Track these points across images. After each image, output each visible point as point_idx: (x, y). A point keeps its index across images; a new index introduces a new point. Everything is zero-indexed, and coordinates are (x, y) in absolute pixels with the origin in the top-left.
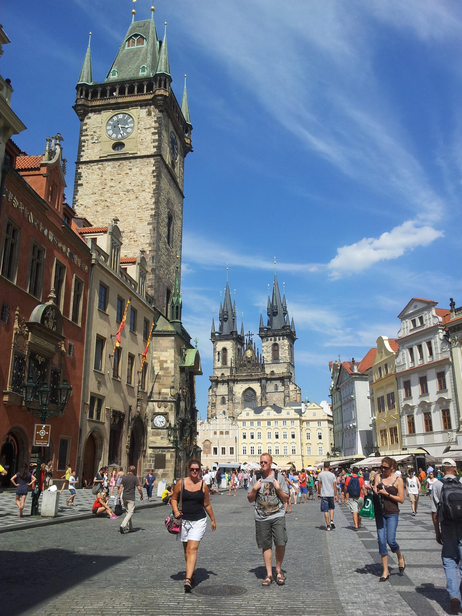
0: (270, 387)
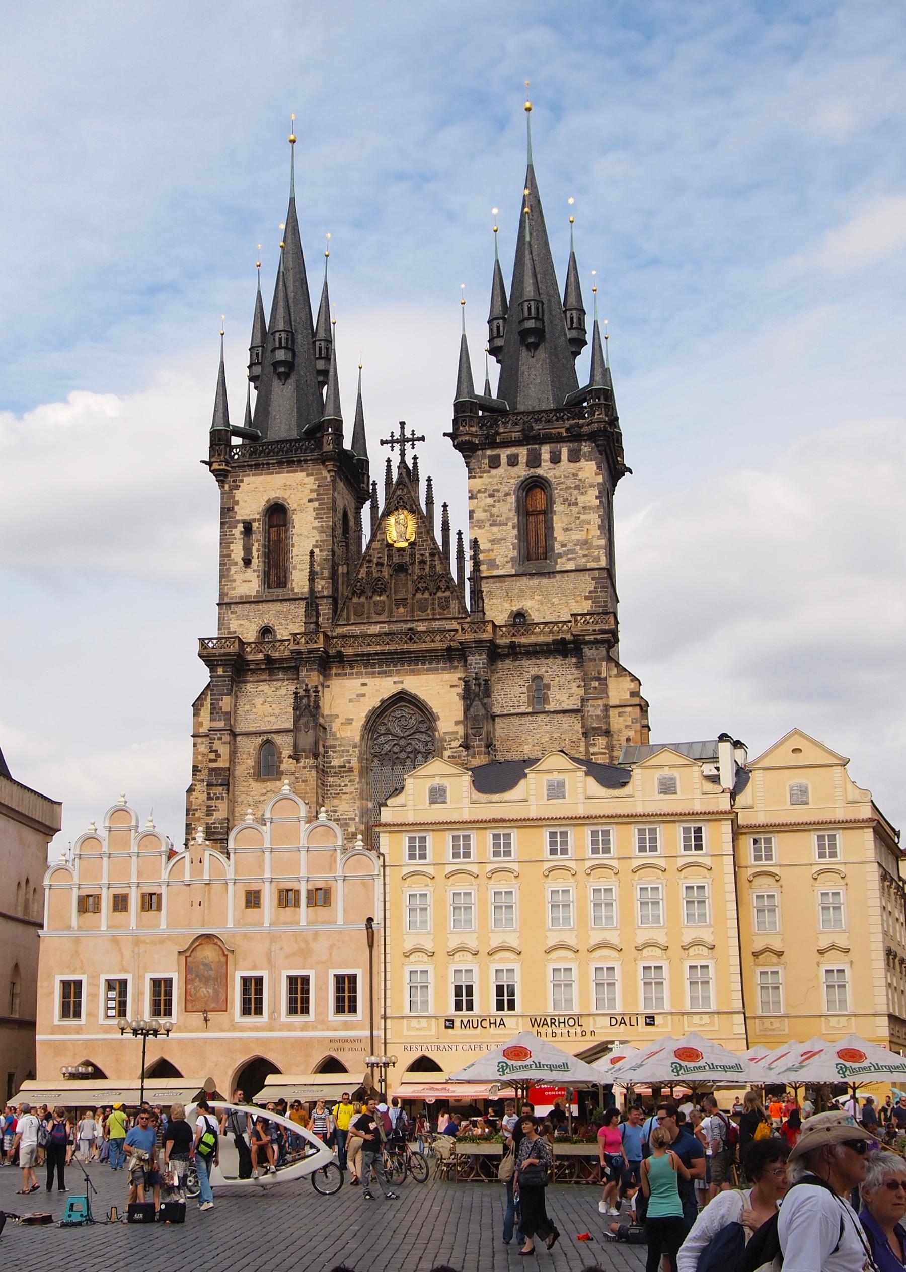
0: (510, 691)
